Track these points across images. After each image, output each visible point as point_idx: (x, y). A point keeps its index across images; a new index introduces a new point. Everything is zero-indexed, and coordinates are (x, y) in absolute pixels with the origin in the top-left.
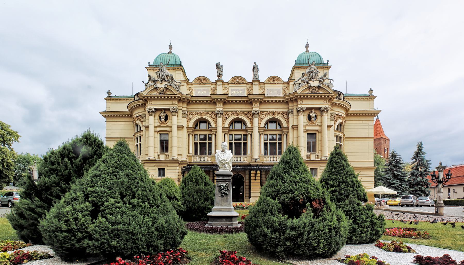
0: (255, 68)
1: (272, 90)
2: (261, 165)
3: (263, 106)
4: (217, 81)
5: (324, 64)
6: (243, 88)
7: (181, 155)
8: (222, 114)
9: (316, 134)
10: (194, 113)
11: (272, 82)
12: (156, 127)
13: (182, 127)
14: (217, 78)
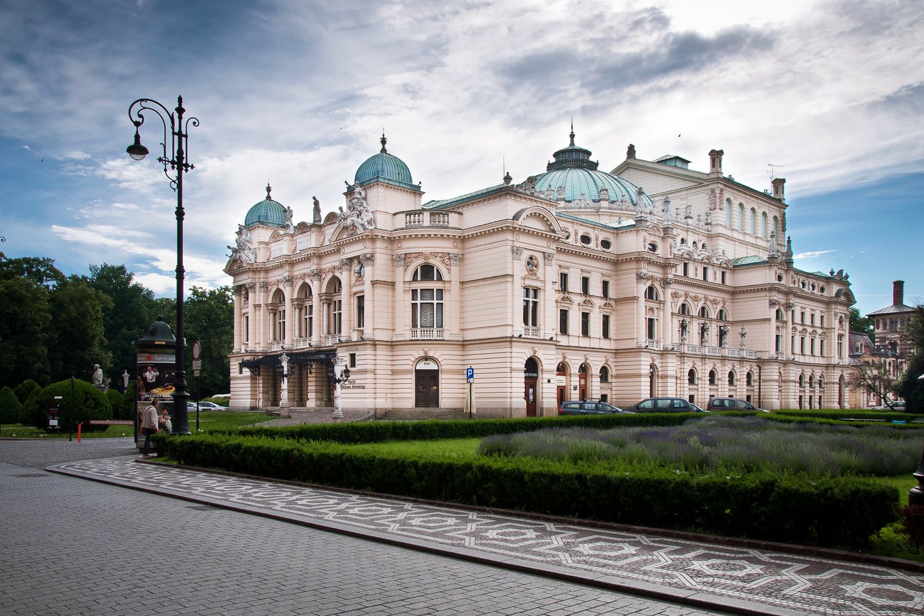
8: (289, 280)
13: (259, 306)
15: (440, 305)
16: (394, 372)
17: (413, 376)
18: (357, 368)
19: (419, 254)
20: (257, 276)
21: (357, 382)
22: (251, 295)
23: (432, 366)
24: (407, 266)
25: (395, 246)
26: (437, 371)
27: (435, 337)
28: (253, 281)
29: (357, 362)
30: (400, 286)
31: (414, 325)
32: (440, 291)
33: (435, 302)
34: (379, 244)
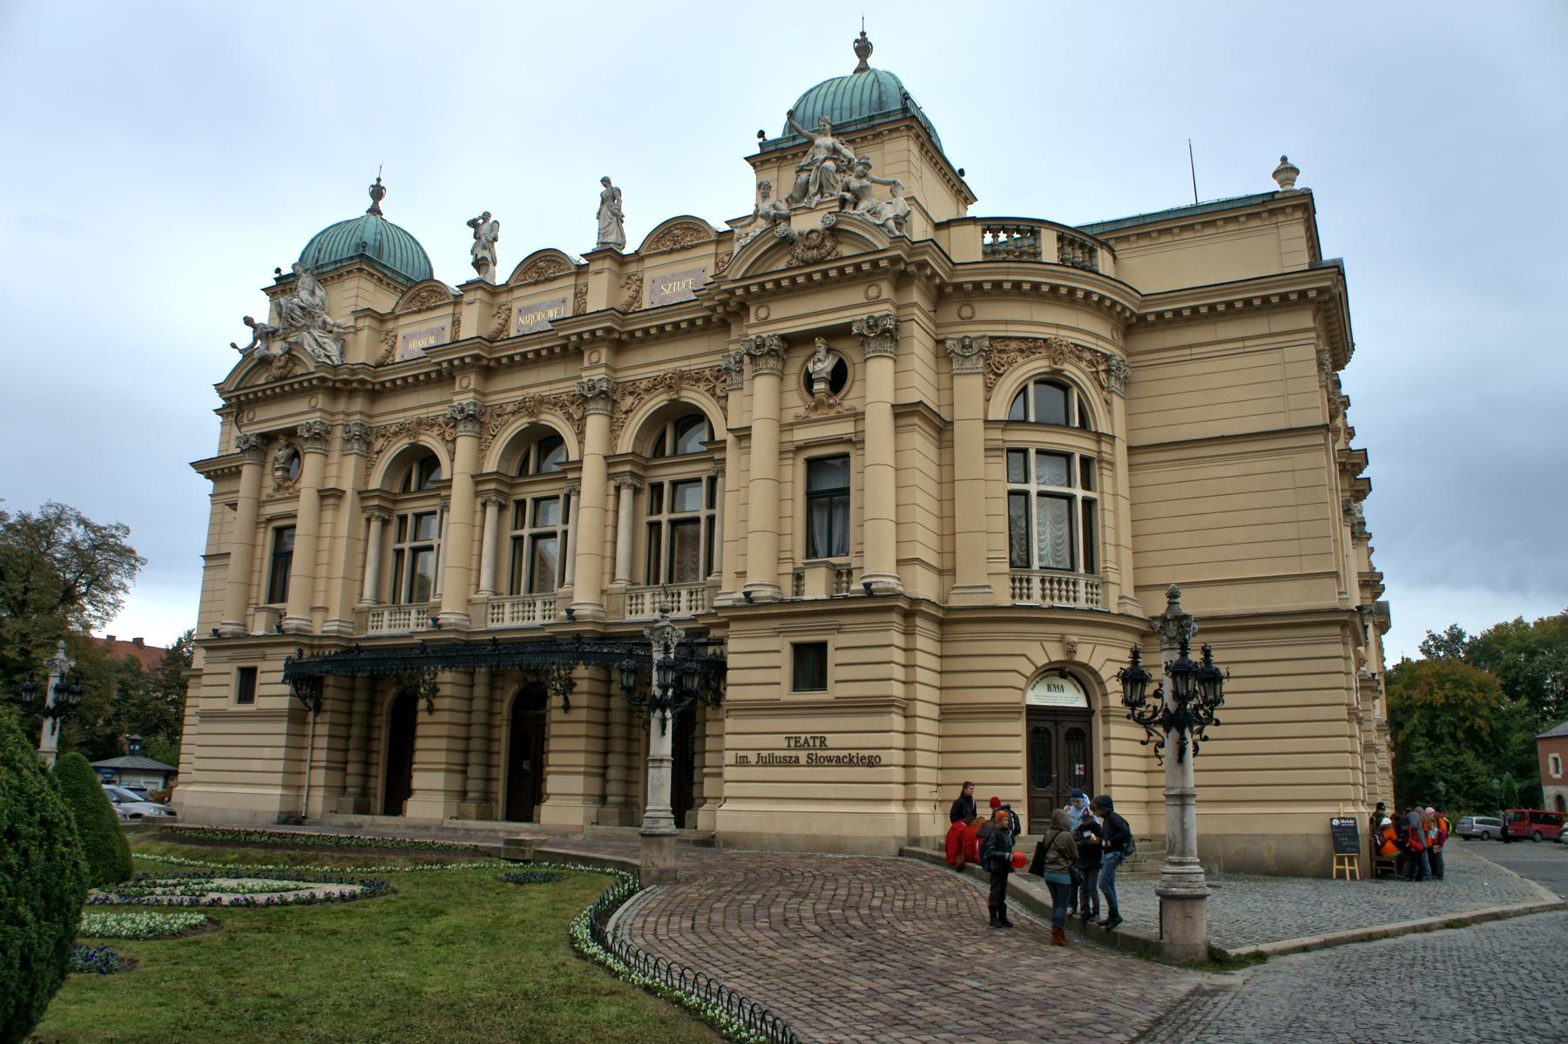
0: (611, 197)
1: (673, 278)
2: (603, 638)
3: (636, 357)
4: (468, 287)
5: (888, 114)
6: (559, 295)
7: (325, 609)
8: (471, 418)
9: (847, 456)
10: (393, 429)
11: (670, 245)
12: (260, 504)
13: (338, 494)
14: (473, 275)
15: (1089, 504)
16: (948, 713)
17: (1020, 726)
18: (835, 691)
19: (1030, 346)
20: (342, 405)
21: (832, 740)
22: (311, 462)
23: (1070, 697)
24: (994, 374)
25: (950, 313)
26: (1086, 714)
27: (1082, 604)
28: (327, 420)
29: (833, 673)
30: (970, 437)
31: (1020, 559)
32: (1086, 462)
33: (1079, 493)
34: (915, 295)
